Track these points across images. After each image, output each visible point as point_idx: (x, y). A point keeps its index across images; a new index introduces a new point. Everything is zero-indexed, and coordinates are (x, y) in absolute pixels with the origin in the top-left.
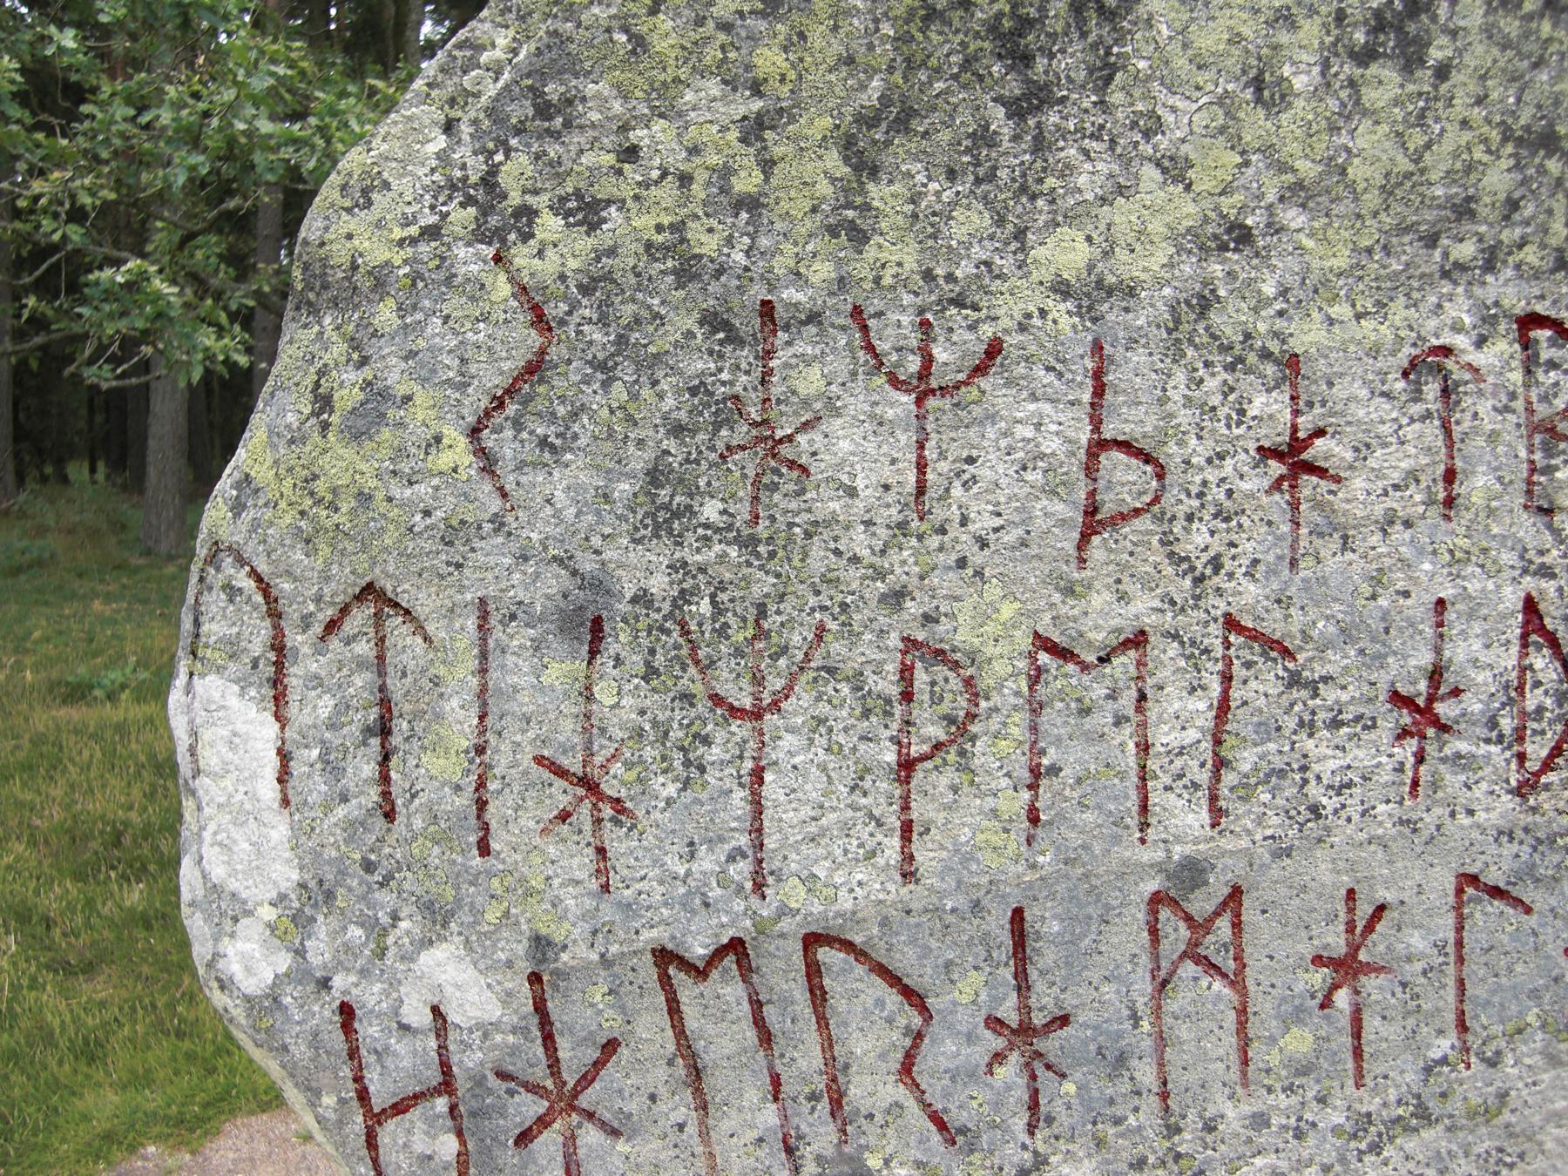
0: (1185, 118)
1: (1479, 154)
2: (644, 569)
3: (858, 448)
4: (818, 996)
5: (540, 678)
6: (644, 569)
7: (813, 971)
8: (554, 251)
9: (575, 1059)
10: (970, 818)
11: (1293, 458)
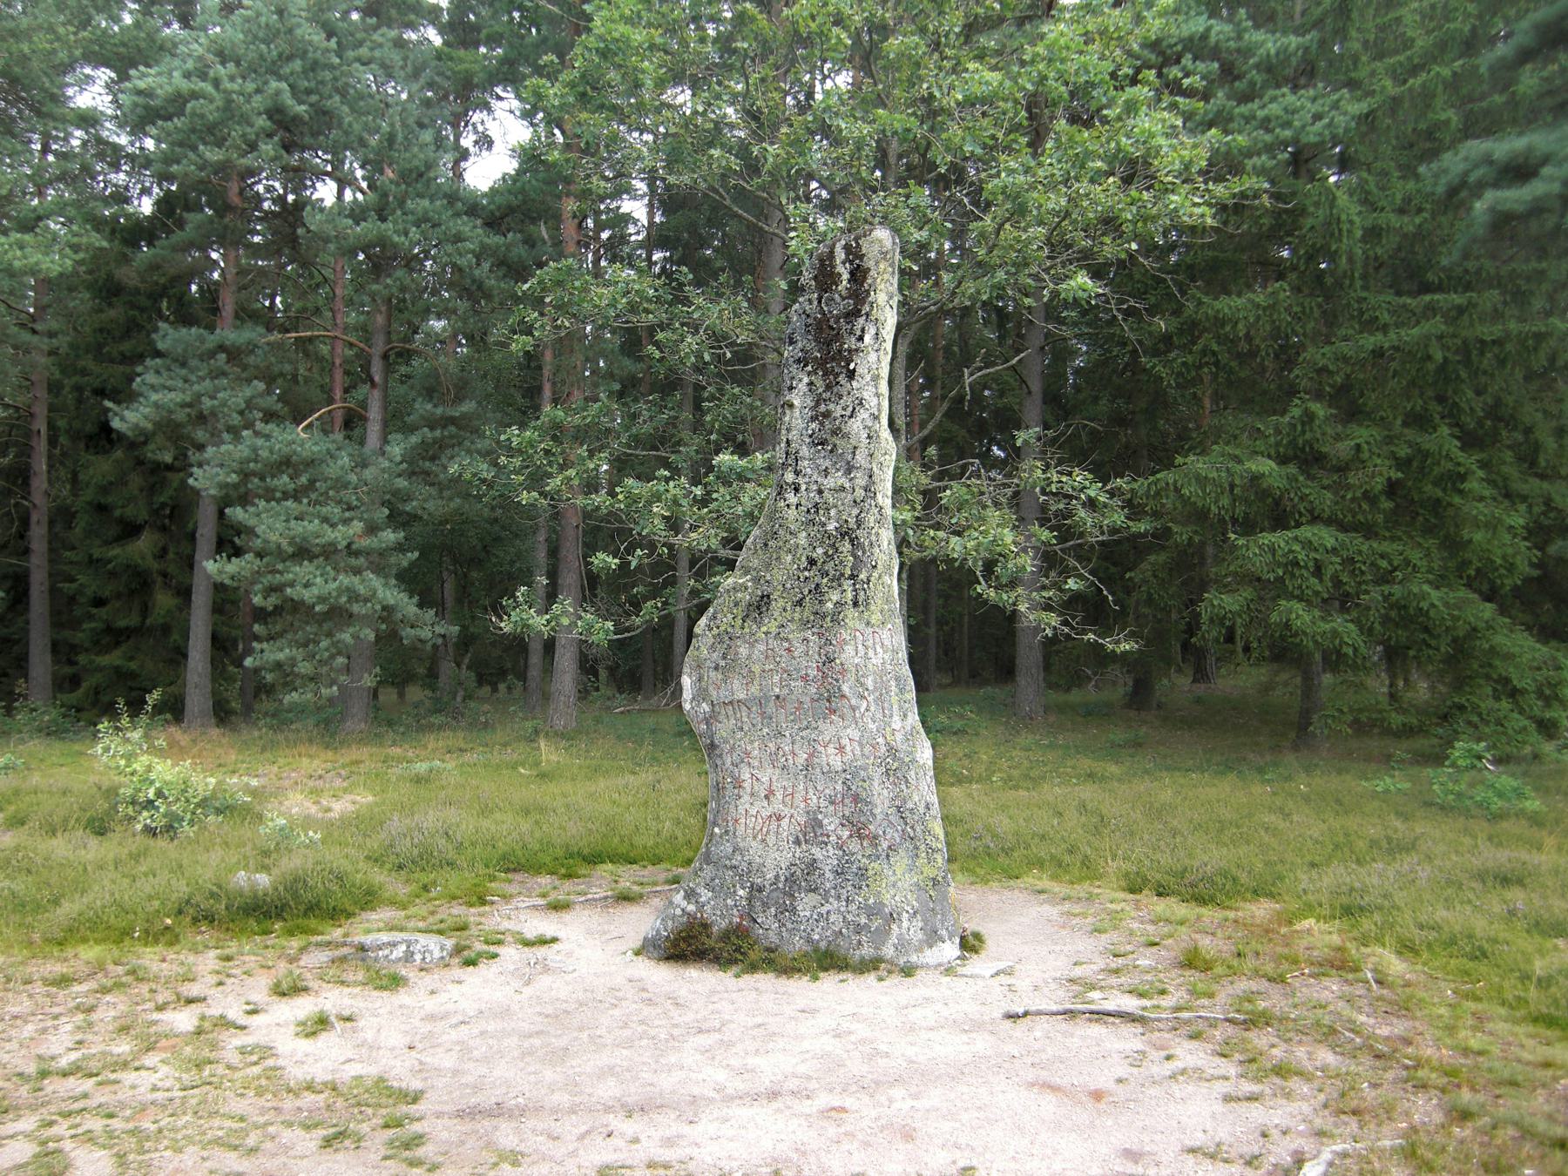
0: (776, 614)
2: (722, 663)
3: (743, 651)
5: (713, 674)
6: (722, 663)
8: (715, 631)
10: (755, 689)
11: (789, 650)
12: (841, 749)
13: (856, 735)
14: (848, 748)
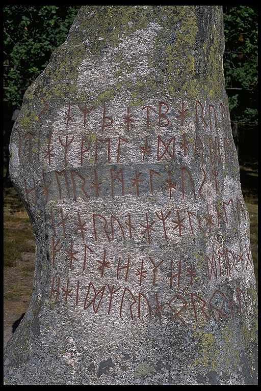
1: (151, 84)
4: (72, 178)
7: (72, 175)
9: (47, 184)
12: (179, 223)
13: (196, 208)
14: (186, 222)
